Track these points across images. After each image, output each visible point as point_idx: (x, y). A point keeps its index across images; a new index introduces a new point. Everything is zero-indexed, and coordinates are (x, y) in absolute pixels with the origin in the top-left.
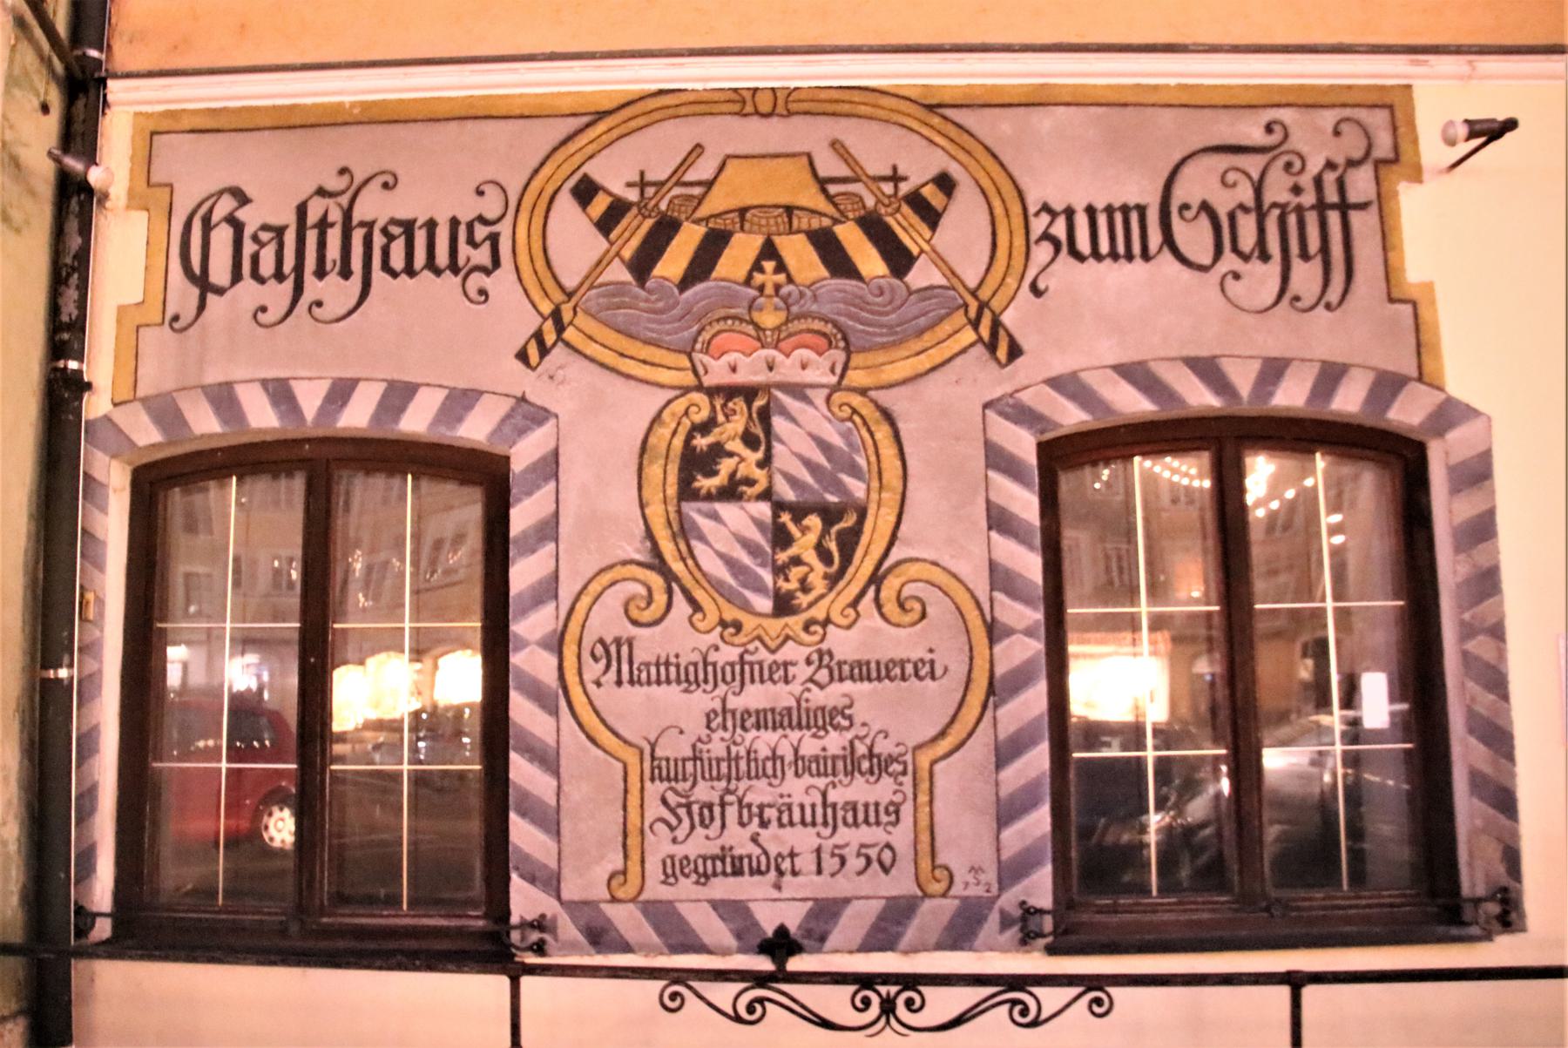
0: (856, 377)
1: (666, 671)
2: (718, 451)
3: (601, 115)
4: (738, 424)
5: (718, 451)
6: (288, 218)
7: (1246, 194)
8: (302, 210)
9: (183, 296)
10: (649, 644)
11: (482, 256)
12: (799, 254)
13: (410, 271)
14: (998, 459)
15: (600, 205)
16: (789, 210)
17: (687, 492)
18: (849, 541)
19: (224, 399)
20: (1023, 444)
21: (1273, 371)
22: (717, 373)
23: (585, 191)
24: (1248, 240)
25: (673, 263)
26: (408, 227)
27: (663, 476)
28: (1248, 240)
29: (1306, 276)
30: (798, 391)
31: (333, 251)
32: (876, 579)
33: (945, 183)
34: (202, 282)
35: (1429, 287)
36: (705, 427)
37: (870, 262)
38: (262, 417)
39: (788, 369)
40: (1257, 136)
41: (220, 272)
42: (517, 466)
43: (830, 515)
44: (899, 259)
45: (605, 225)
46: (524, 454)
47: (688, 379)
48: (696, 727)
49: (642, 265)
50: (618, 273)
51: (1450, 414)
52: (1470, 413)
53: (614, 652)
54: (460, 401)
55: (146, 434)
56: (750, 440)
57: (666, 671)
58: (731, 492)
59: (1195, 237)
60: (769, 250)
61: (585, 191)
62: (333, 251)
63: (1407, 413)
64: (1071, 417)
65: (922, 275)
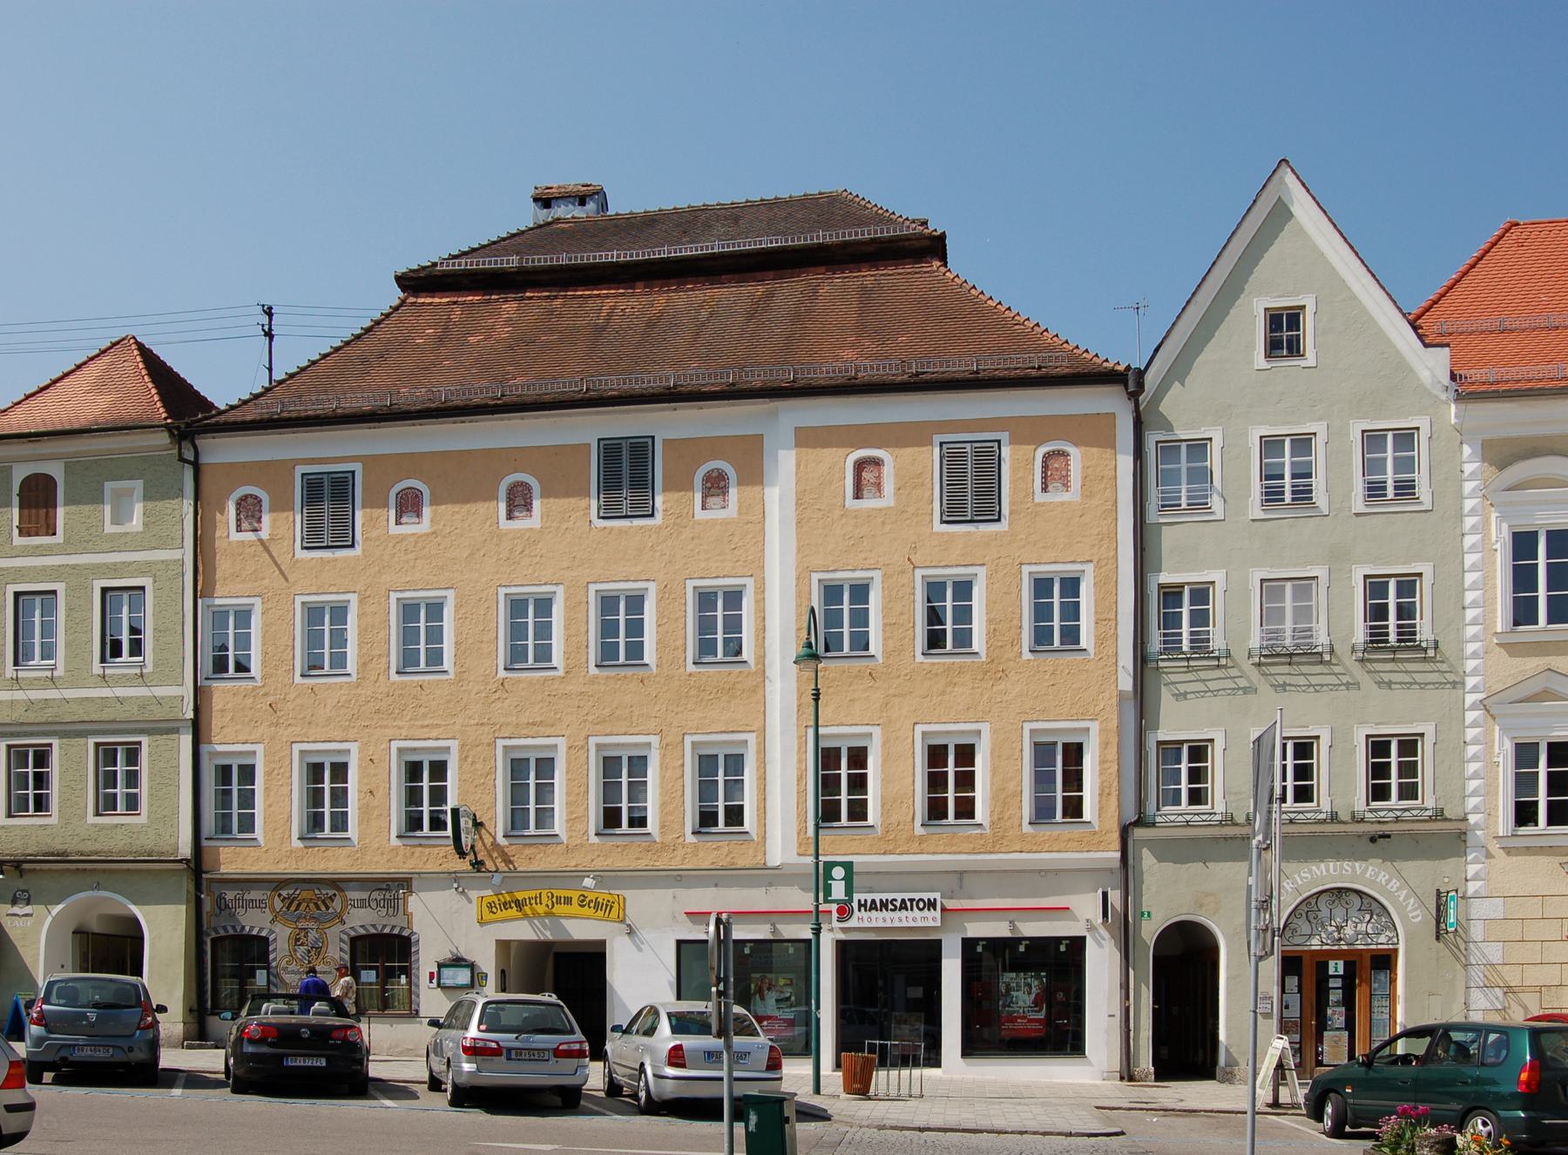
0: (321, 927)
1: (293, 972)
2: (300, 938)
3: (281, 882)
4: (303, 934)
5: (300, 938)
6: (233, 898)
7: (382, 897)
8: (235, 896)
9: (217, 911)
10: (291, 968)
11: (264, 906)
12: (311, 905)
13: (253, 908)
14: (341, 940)
15: (282, 897)
16: (311, 899)
17: (296, 945)
18: (319, 953)
19: (225, 928)
20: (345, 938)
21: (384, 926)
22: (300, 925)
23: (280, 895)
24: (382, 905)
25: (293, 908)
26: (252, 900)
27: (291, 941)
28: (382, 905)
29: (391, 910)
30: (312, 929)
31: (241, 904)
32: (323, 959)
33: (335, 895)
34: (220, 908)
35: (412, 913)
36: (298, 935)
37: (323, 909)
38: (231, 932)
39: (310, 926)
40: (384, 887)
41: (223, 907)
42: (270, 940)
43: (317, 948)
44: (327, 908)
45: (283, 901)
46: (271, 938)
47: (295, 926)
48: (297, 981)
49: (288, 908)
50: (284, 909)
51: (412, 933)
52: (416, 934)
53: (285, 969)
54: (261, 929)
55: (214, 935)
56: (305, 937)
57: (293, 972)
58: (302, 945)
59: (373, 904)
60: (308, 906)
61: (280, 895)
62: (241, 904)
63: (406, 933)
64: (353, 934)
65: (331, 910)
